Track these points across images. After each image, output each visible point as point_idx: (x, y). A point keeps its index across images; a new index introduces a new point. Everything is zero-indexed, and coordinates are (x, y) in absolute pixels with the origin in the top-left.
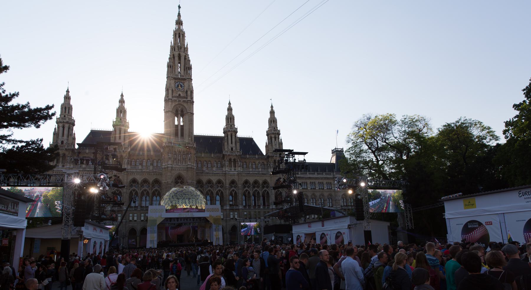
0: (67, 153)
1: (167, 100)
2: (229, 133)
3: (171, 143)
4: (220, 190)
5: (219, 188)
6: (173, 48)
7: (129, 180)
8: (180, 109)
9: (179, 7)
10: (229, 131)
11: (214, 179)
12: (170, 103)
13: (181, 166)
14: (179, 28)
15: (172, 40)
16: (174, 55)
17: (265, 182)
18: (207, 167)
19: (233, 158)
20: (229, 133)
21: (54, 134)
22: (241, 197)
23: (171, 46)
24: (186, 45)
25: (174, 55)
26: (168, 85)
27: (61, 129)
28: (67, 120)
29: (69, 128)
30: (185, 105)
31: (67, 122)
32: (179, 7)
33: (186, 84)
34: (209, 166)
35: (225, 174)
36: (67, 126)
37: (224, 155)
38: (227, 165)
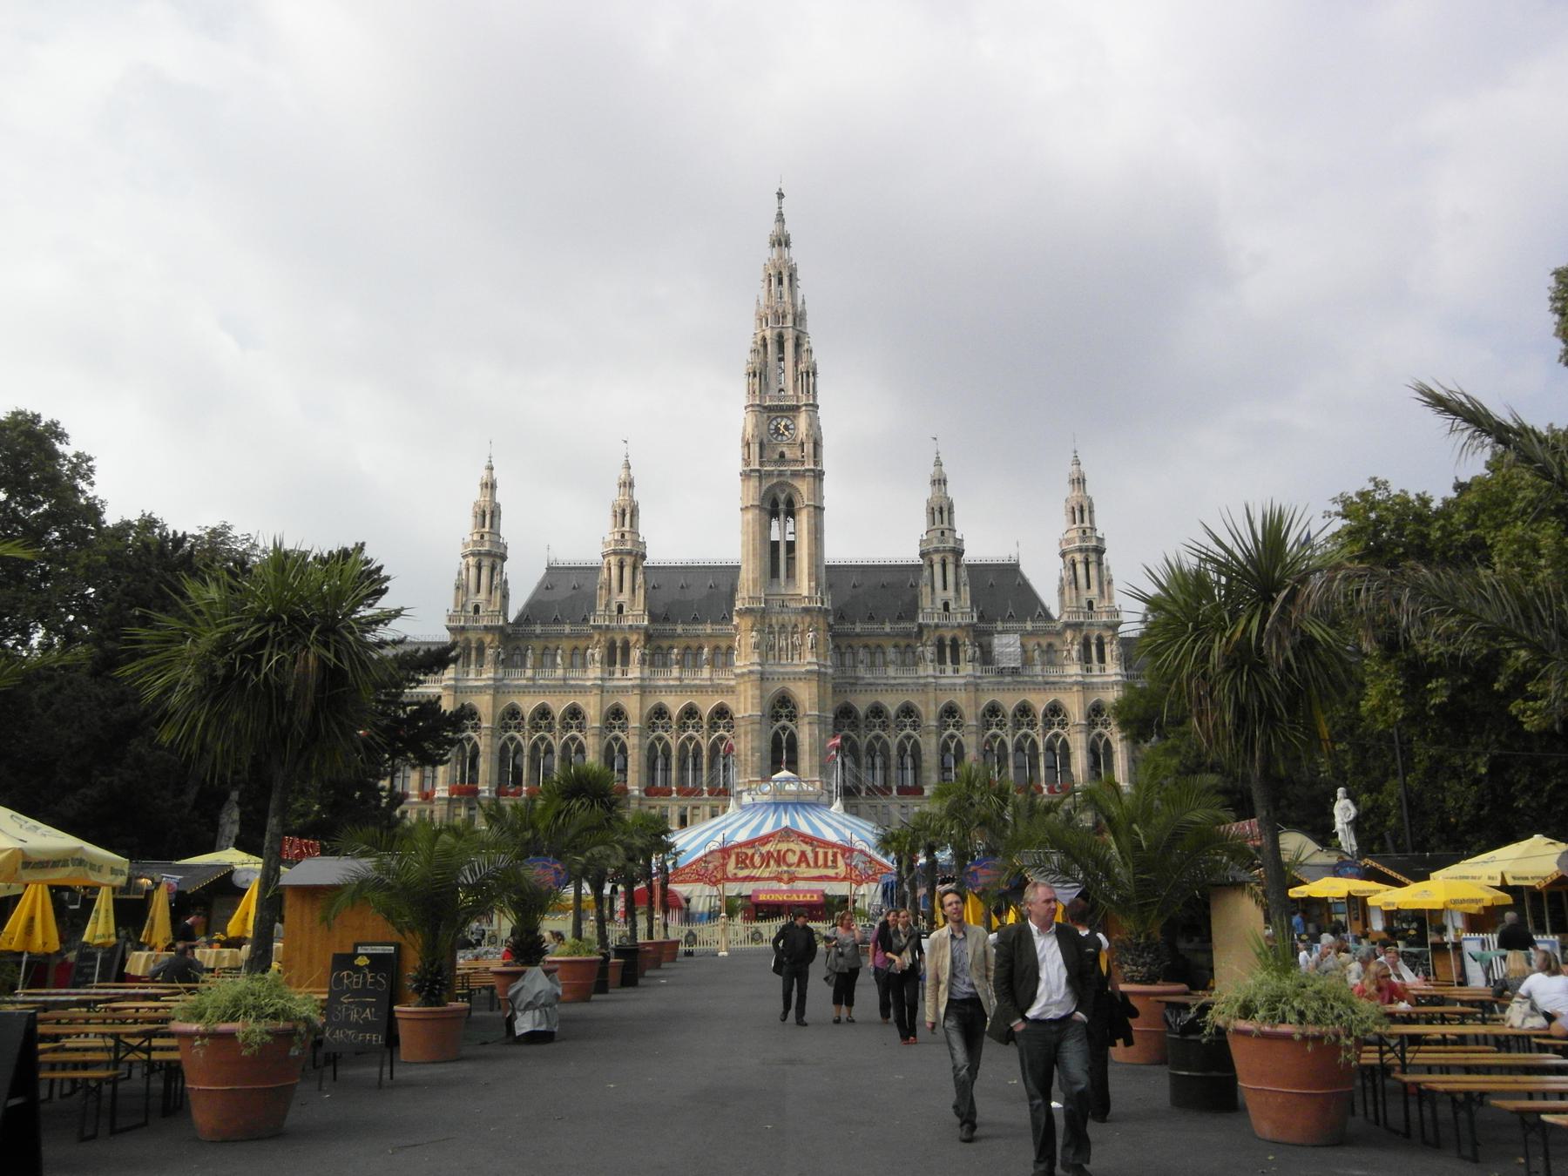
0: (488, 639)
1: (746, 475)
2: (937, 558)
4: (909, 737)
6: (763, 319)
8: (782, 497)
9: (781, 195)
10: (937, 551)
11: (892, 703)
12: (754, 483)
13: (789, 669)
15: (763, 293)
16: (764, 339)
17: (1055, 710)
18: (873, 664)
19: (948, 636)
20: (937, 558)
24: (800, 302)
25: (764, 339)
26: (750, 430)
27: (473, 571)
28: (487, 547)
29: (493, 569)
31: (488, 554)
32: (781, 195)
33: (802, 421)
35: (925, 685)
37: (921, 627)
38: (929, 656)
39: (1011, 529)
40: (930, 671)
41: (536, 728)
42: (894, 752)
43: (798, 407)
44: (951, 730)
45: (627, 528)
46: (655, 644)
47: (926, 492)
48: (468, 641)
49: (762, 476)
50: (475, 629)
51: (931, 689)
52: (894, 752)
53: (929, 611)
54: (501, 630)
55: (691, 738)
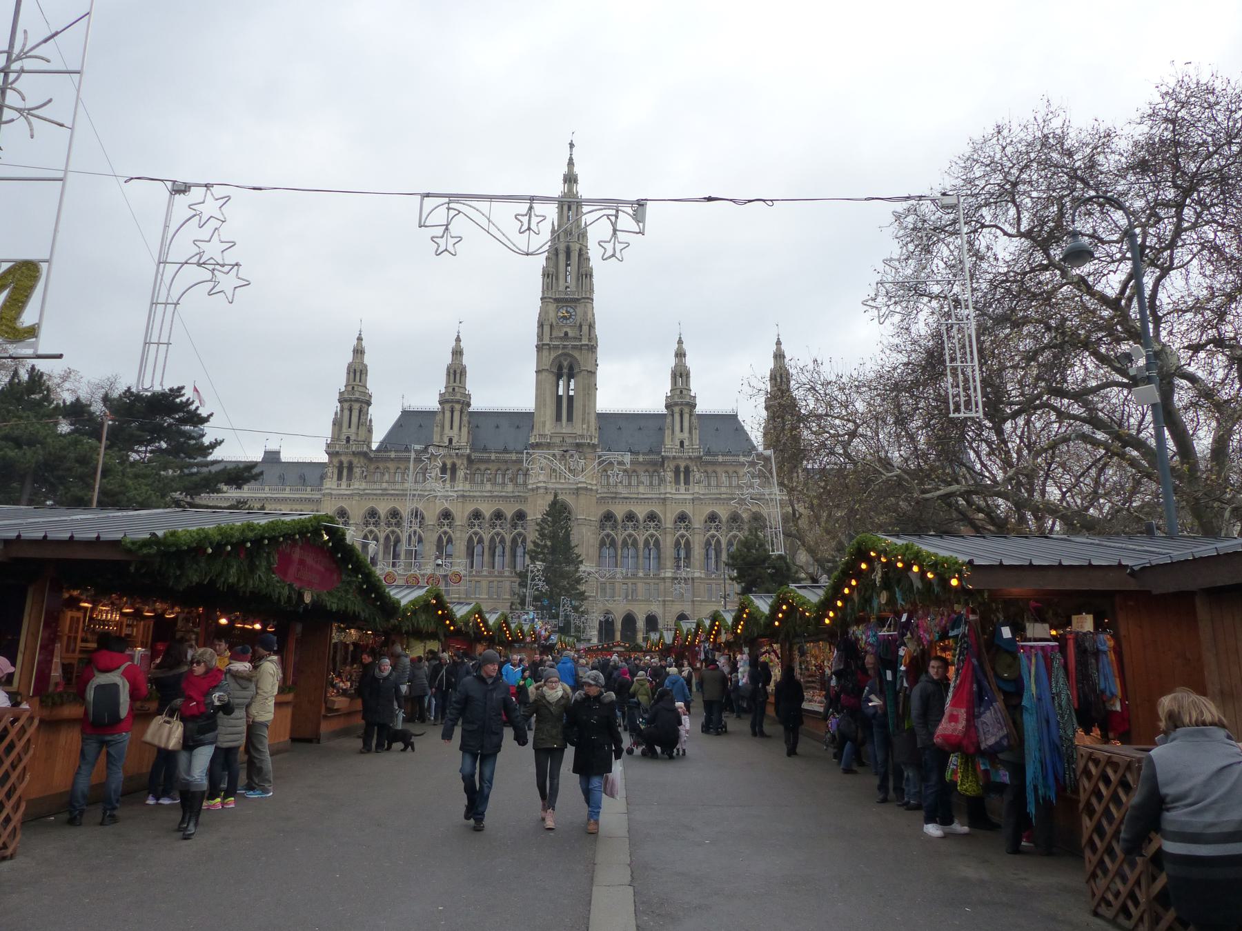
0: (355, 461)
1: (539, 348)
2: (677, 409)
3: (544, 436)
4: (652, 536)
5: (652, 531)
7: (466, 514)
8: (565, 364)
9: (572, 145)
10: (676, 404)
11: (641, 512)
12: (545, 353)
14: (570, 190)
16: (556, 250)
18: (630, 484)
20: (677, 409)
21: (334, 424)
22: (698, 551)
23: (553, 232)
25: (556, 250)
27: (346, 413)
29: (360, 411)
30: (576, 354)
31: (357, 400)
33: (580, 310)
34: (634, 482)
35: (664, 499)
36: (356, 406)
37: (663, 458)
38: (668, 479)
39: (732, 388)
40: (669, 490)
41: (389, 524)
42: (641, 545)
43: (578, 300)
44: (683, 531)
45: (458, 383)
46: (475, 467)
47: (671, 362)
48: (341, 463)
49: (551, 348)
50: (346, 454)
51: (668, 502)
52: (641, 545)
53: (670, 446)
54: (365, 455)
55: (498, 534)
